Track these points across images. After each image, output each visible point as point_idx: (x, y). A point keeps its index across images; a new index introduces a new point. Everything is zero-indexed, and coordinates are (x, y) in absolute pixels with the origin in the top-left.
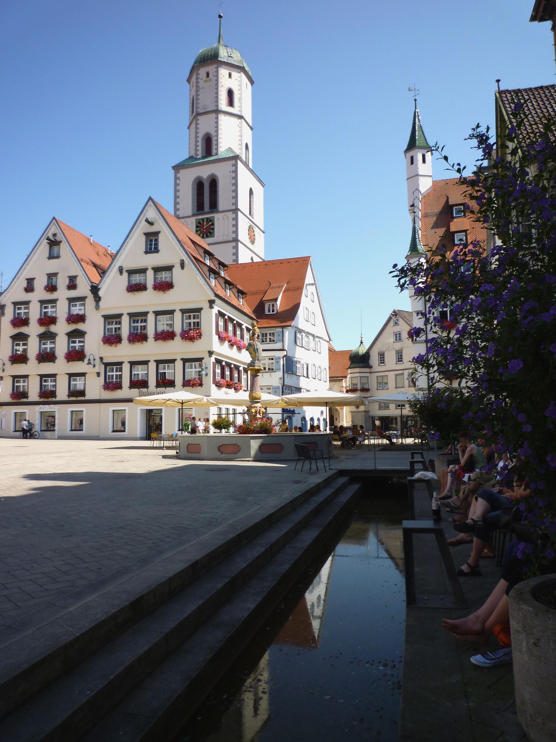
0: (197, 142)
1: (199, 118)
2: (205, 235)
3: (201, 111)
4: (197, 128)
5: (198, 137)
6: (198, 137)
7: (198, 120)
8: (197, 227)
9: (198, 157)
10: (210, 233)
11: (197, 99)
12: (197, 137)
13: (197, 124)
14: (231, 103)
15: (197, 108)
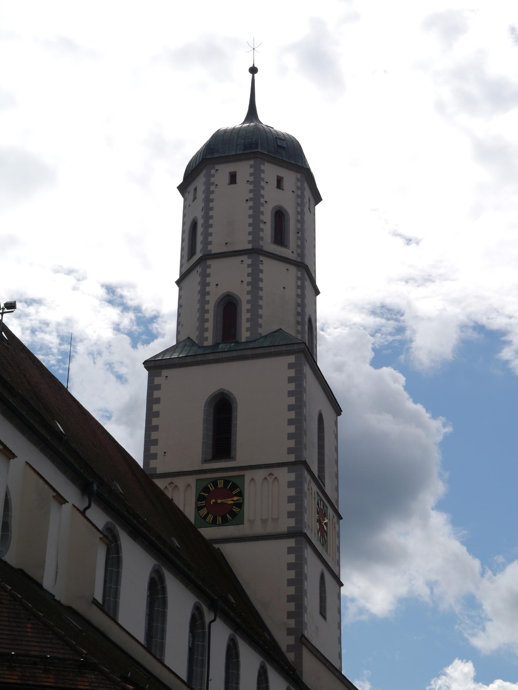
0: (203, 311)
1: (209, 262)
2: (219, 519)
3: (215, 249)
4: (204, 284)
5: (208, 302)
6: (208, 302)
7: (209, 267)
8: (200, 498)
9: (206, 344)
10: (234, 515)
11: (207, 226)
12: (203, 302)
13: (205, 275)
14: (280, 236)
15: (206, 243)
